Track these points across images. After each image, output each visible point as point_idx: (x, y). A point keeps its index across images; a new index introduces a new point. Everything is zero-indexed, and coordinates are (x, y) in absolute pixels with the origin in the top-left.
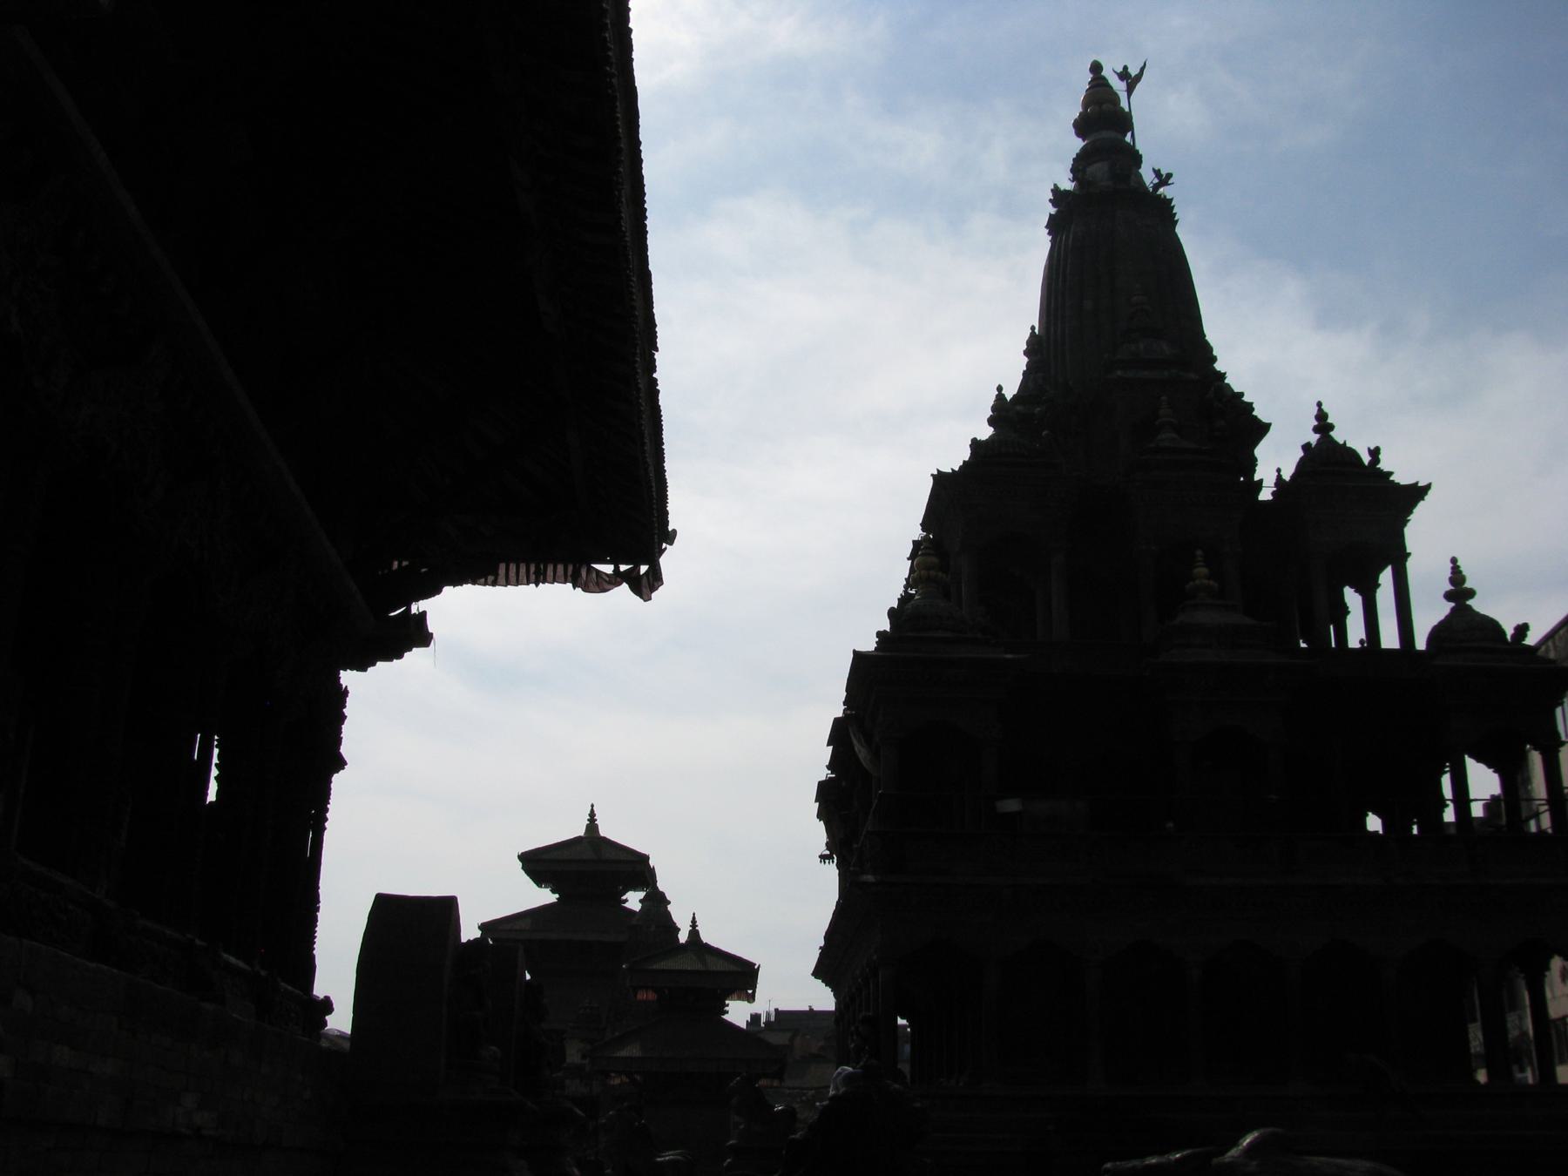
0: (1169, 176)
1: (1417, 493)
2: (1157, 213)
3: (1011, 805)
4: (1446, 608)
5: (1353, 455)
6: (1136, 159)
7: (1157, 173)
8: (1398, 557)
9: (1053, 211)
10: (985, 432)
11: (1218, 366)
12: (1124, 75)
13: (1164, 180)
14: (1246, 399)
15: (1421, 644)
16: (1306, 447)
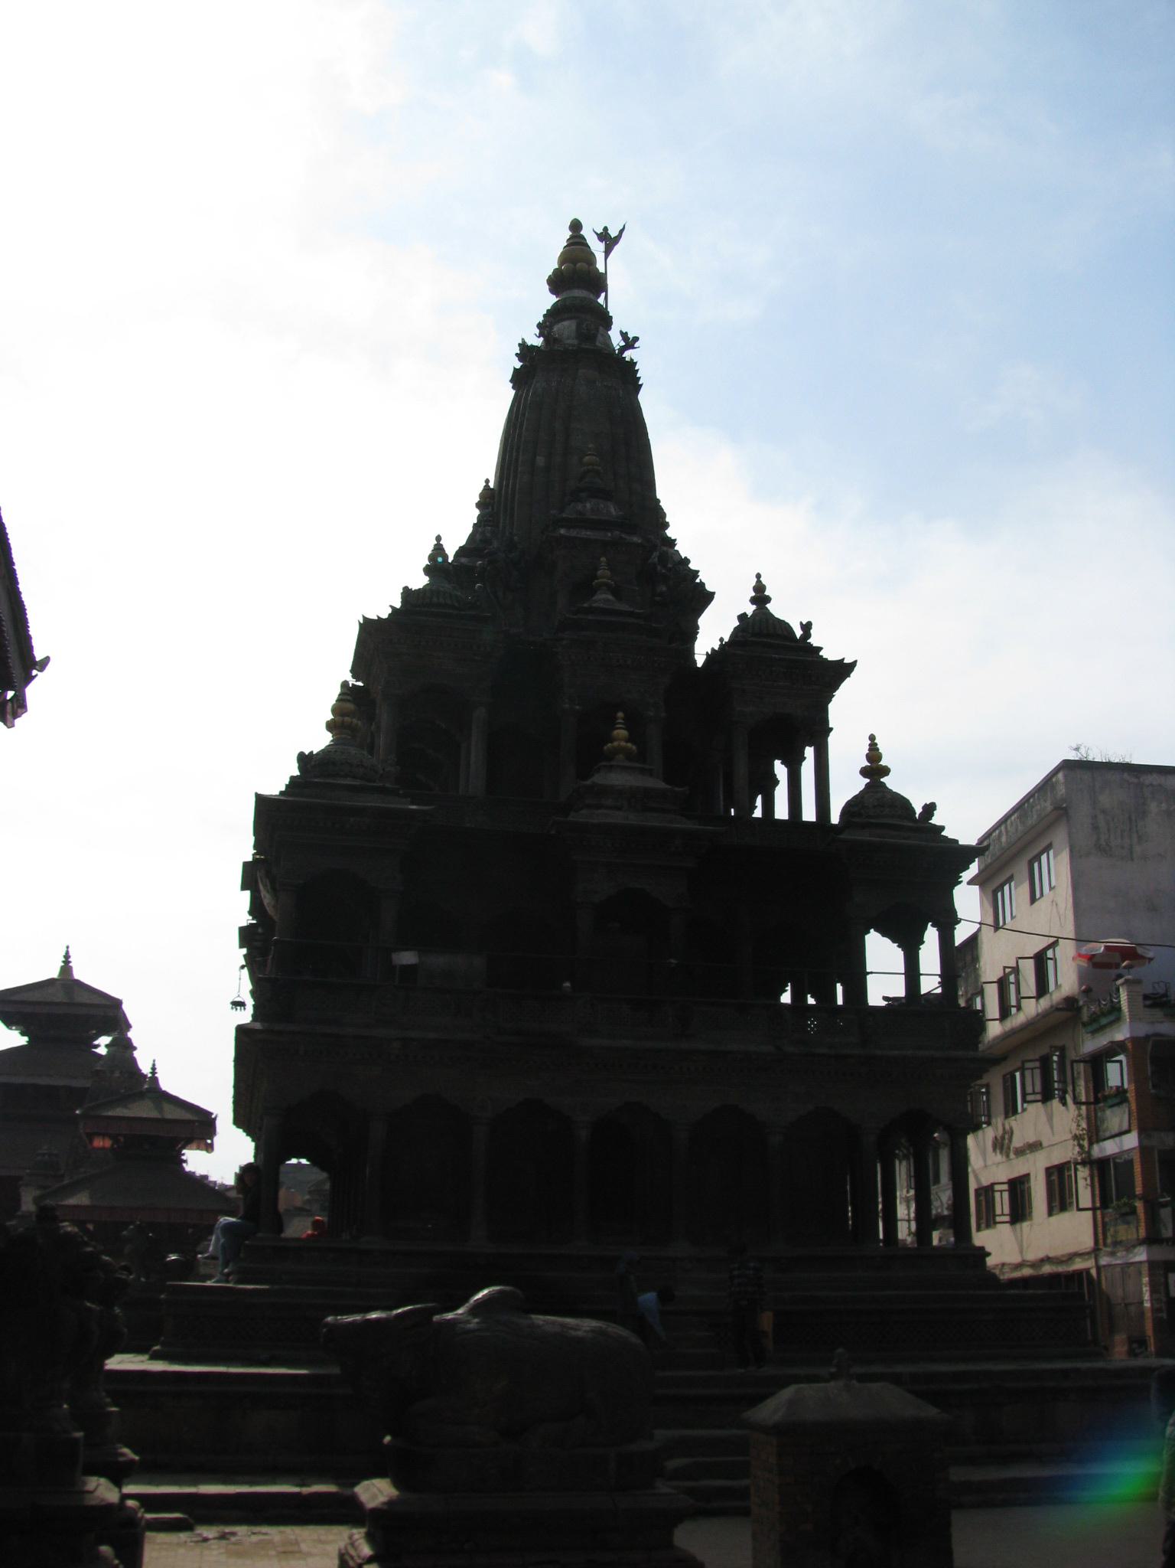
0: (636, 339)
2: (624, 377)
3: (407, 958)
5: (785, 627)
6: (606, 321)
7: (624, 335)
8: (818, 732)
9: (518, 365)
12: (604, 236)
13: (630, 343)
14: (692, 566)
15: (835, 819)
16: (742, 617)
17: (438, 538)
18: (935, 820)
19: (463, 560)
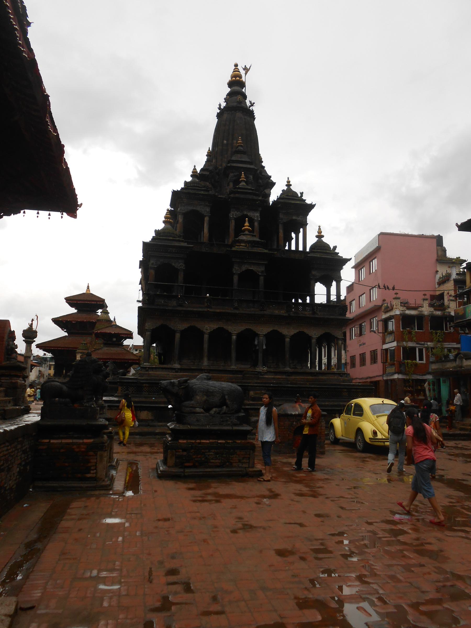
1: (312, 206)
2: (250, 115)
4: (316, 239)
5: (296, 193)
6: (245, 97)
7: (250, 102)
8: (304, 225)
10: (189, 179)
11: (263, 164)
15: (308, 250)
17: (195, 166)
18: (337, 251)
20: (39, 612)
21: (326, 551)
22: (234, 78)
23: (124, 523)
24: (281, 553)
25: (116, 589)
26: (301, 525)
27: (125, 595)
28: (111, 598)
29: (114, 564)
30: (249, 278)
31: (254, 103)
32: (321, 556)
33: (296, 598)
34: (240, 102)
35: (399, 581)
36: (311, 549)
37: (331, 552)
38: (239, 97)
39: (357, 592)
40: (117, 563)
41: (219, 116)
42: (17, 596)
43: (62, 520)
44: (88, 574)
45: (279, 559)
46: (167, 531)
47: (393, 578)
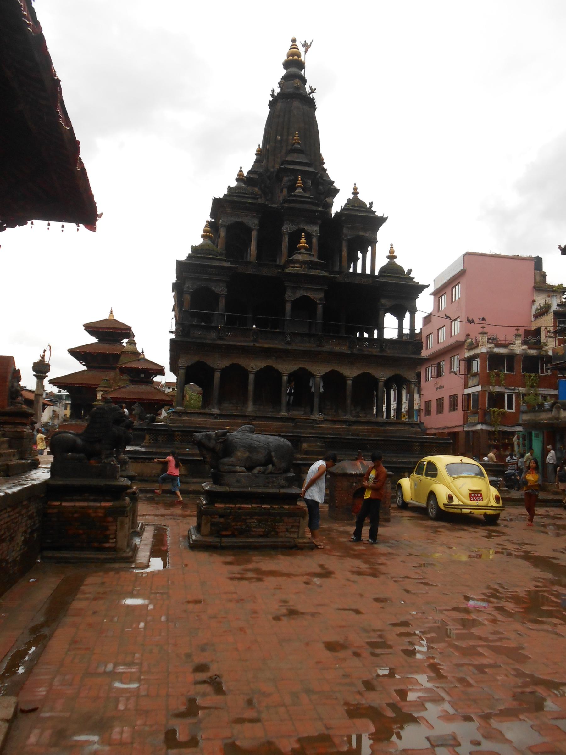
2: (310, 104)
4: (386, 261)
5: (363, 203)
6: (304, 81)
7: (311, 88)
8: (373, 242)
10: (234, 184)
15: (377, 273)
16: (348, 200)
17: (241, 168)
18: (412, 275)
19: (252, 176)
20: (43, 715)
21: (384, 645)
22: (291, 57)
23: (147, 605)
24: (331, 647)
25: (134, 688)
26: (358, 612)
27: (145, 696)
28: (128, 699)
29: (134, 657)
30: (304, 306)
31: (315, 89)
32: (378, 651)
33: (346, 704)
34: (298, 88)
35: (469, 685)
36: (367, 643)
37: (390, 647)
38: (297, 81)
39: (419, 698)
40: (137, 655)
41: (271, 104)
42: (17, 695)
43: (73, 600)
44: (101, 669)
45: (328, 654)
46: (198, 616)
47: (462, 680)
